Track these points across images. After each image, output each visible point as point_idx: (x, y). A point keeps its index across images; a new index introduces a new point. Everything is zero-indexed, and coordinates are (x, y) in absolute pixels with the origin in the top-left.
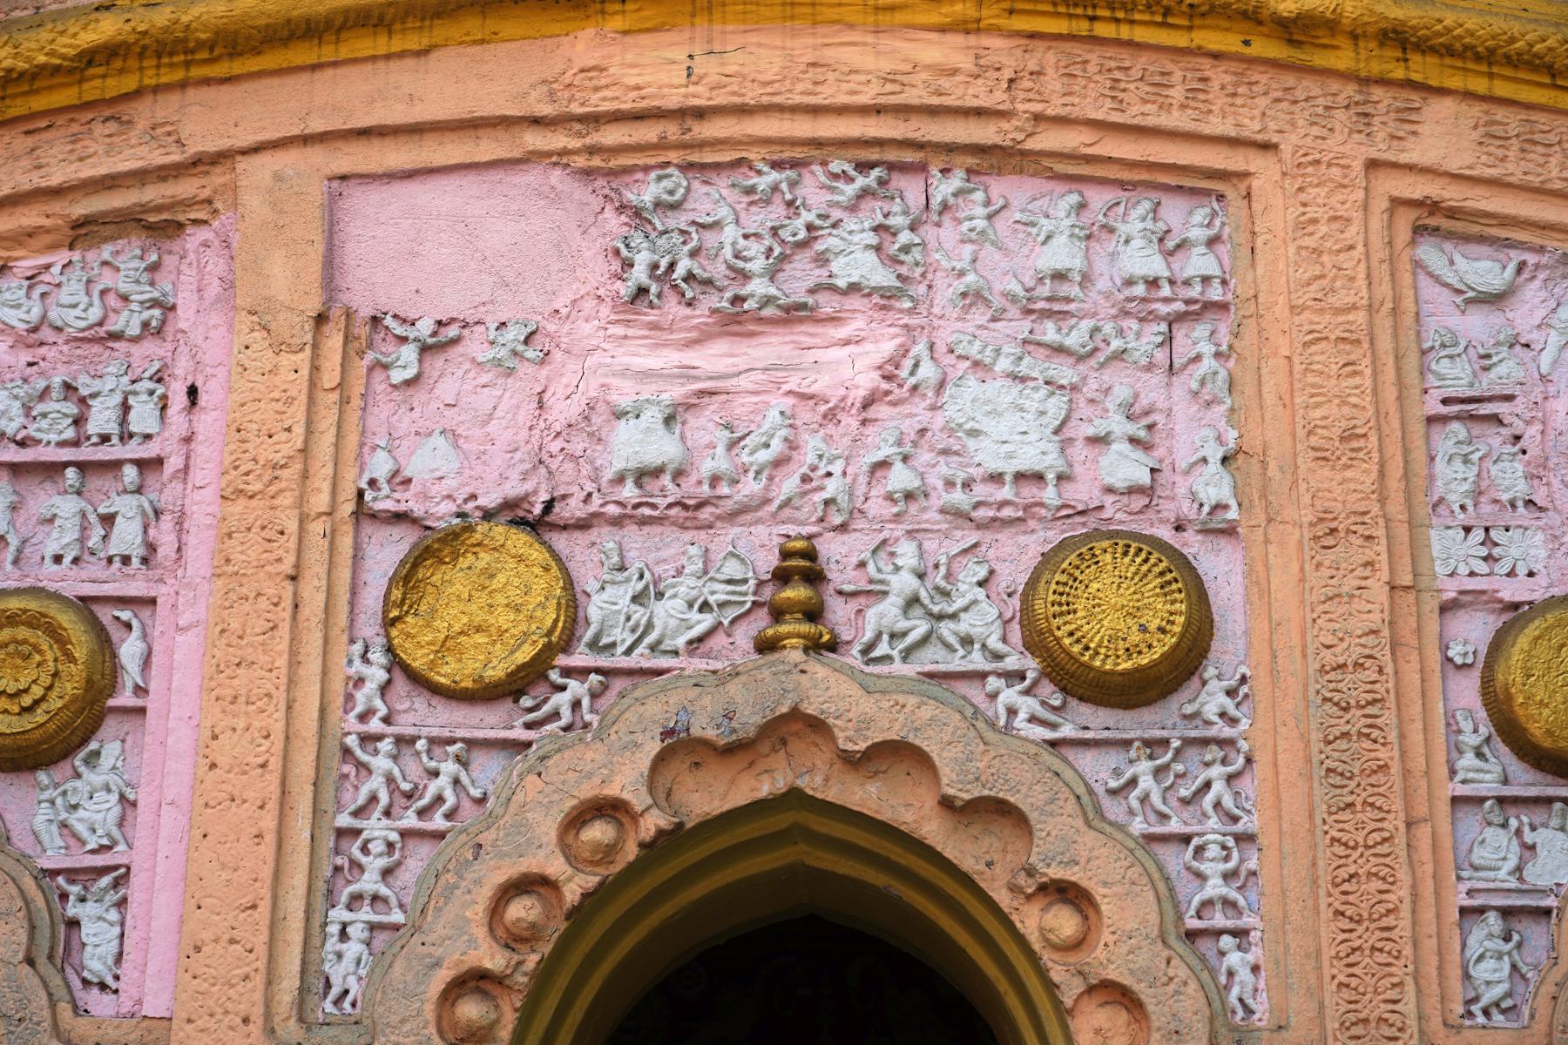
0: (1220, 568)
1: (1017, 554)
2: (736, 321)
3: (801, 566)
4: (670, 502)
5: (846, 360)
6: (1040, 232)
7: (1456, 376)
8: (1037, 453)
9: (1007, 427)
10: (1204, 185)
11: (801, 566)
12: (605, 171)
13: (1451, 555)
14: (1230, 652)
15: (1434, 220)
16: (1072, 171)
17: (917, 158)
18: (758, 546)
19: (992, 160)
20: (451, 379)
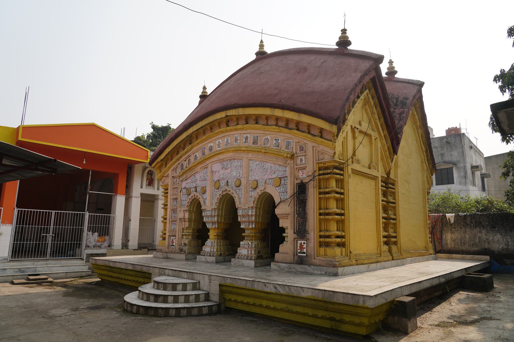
0: (242, 179)
1: (235, 180)
2: (226, 169)
3: (227, 182)
4: (223, 179)
5: (229, 171)
6: (236, 163)
7: (251, 168)
8: (235, 175)
9: (234, 173)
10: (240, 159)
11: (227, 182)
12: (221, 162)
13: (250, 178)
14: (242, 184)
15: (250, 160)
16: (237, 159)
17: (230, 160)
18: (226, 180)
19: (234, 159)
20: (216, 174)
